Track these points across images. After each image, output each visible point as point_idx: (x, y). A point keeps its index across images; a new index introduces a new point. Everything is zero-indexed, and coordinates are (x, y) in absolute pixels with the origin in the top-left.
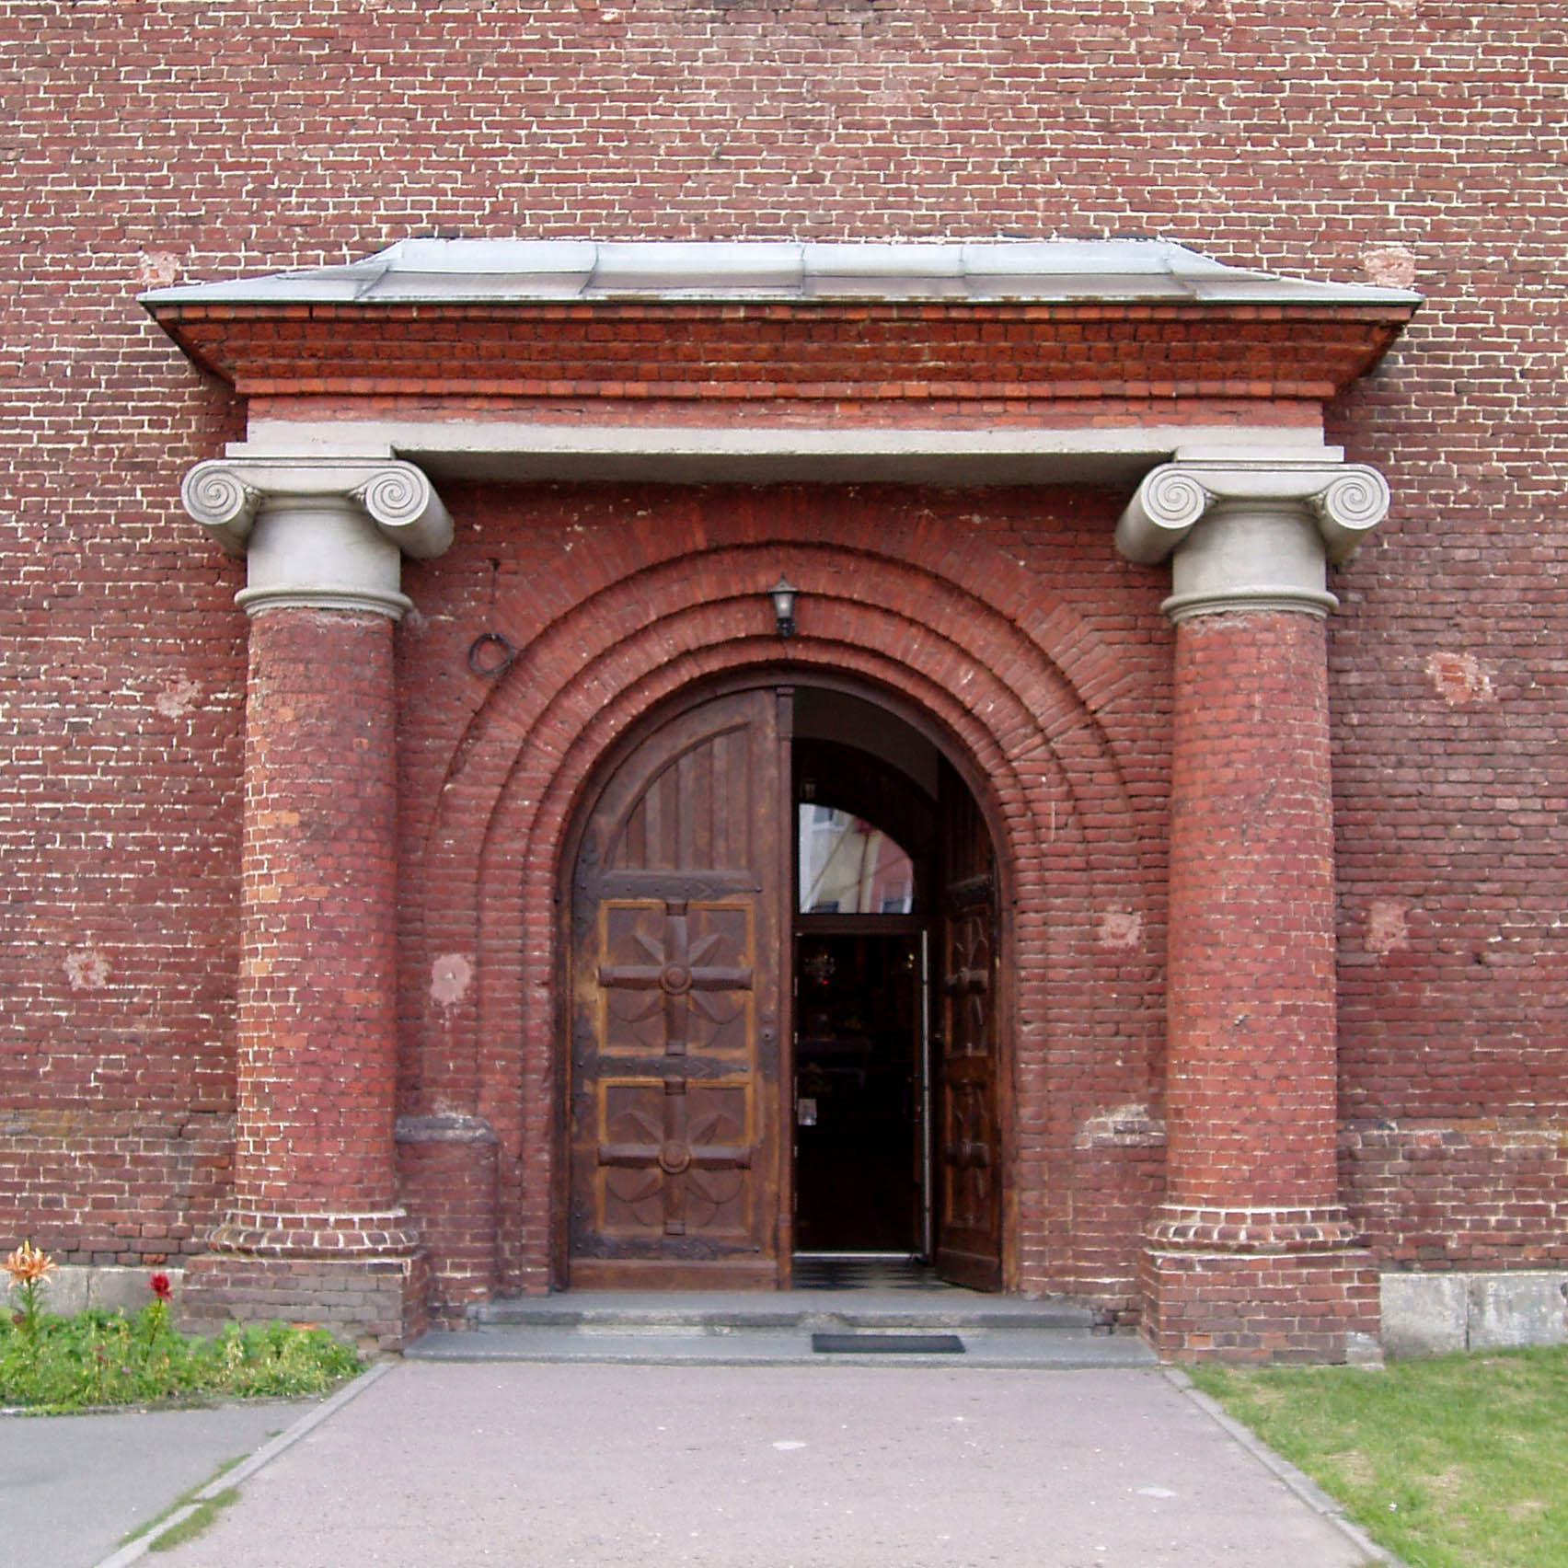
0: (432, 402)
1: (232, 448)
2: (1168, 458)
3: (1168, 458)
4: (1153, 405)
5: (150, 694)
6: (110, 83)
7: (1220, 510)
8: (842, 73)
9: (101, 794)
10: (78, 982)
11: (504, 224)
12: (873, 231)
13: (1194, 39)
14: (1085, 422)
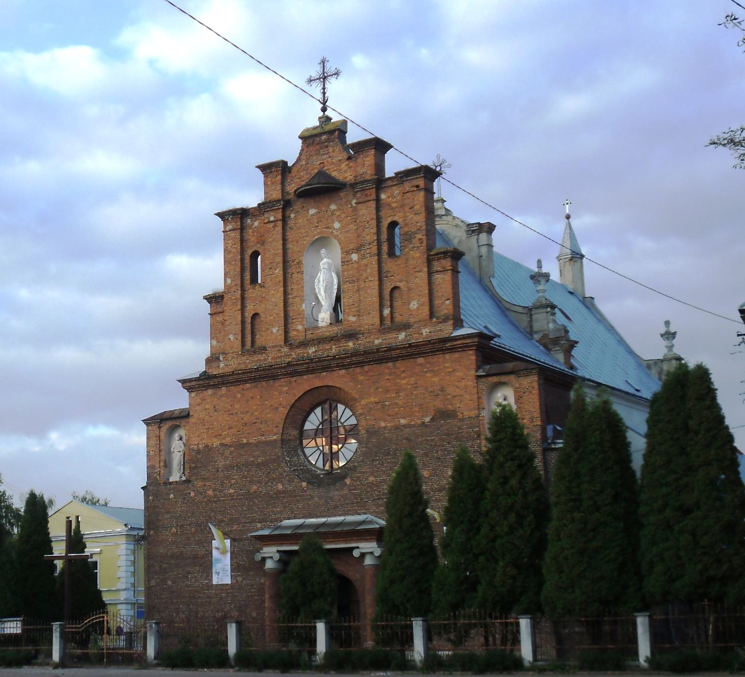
0: (281, 544)
1: (261, 551)
2: (358, 548)
3: (358, 548)
4: (357, 541)
5: (260, 579)
6: (253, 502)
7: (363, 555)
8: (331, 495)
9: (255, 592)
10: (253, 616)
11: (295, 518)
12: (335, 516)
13: (370, 486)
14: (350, 543)
